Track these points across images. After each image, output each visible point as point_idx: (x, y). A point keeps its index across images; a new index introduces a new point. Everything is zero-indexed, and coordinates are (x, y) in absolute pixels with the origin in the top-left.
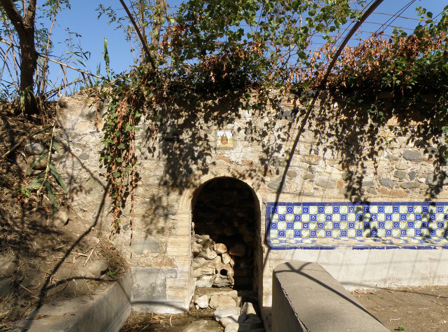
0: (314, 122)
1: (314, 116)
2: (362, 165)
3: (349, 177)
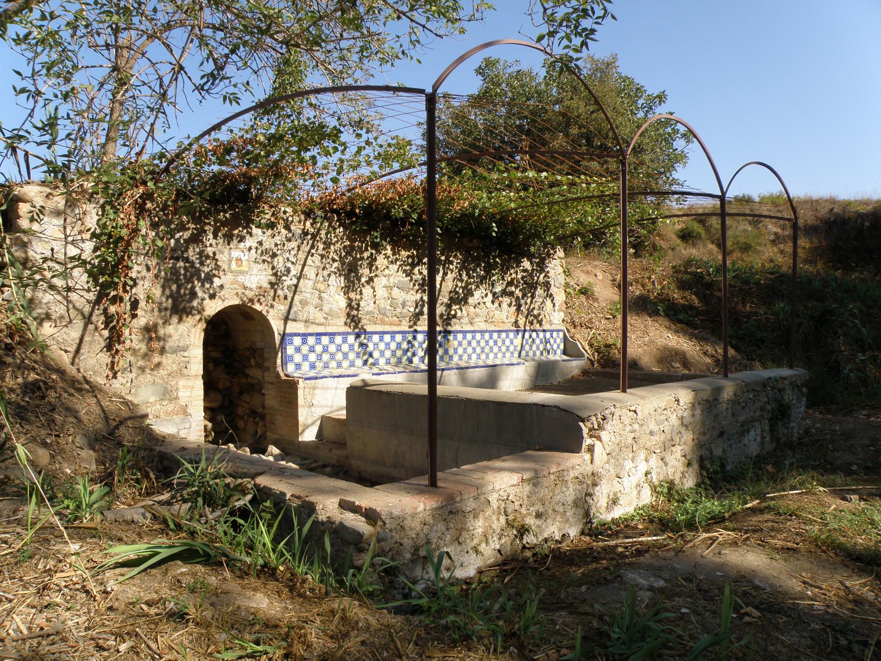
0: (321, 246)
1: (321, 239)
2: (361, 291)
3: (349, 305)
